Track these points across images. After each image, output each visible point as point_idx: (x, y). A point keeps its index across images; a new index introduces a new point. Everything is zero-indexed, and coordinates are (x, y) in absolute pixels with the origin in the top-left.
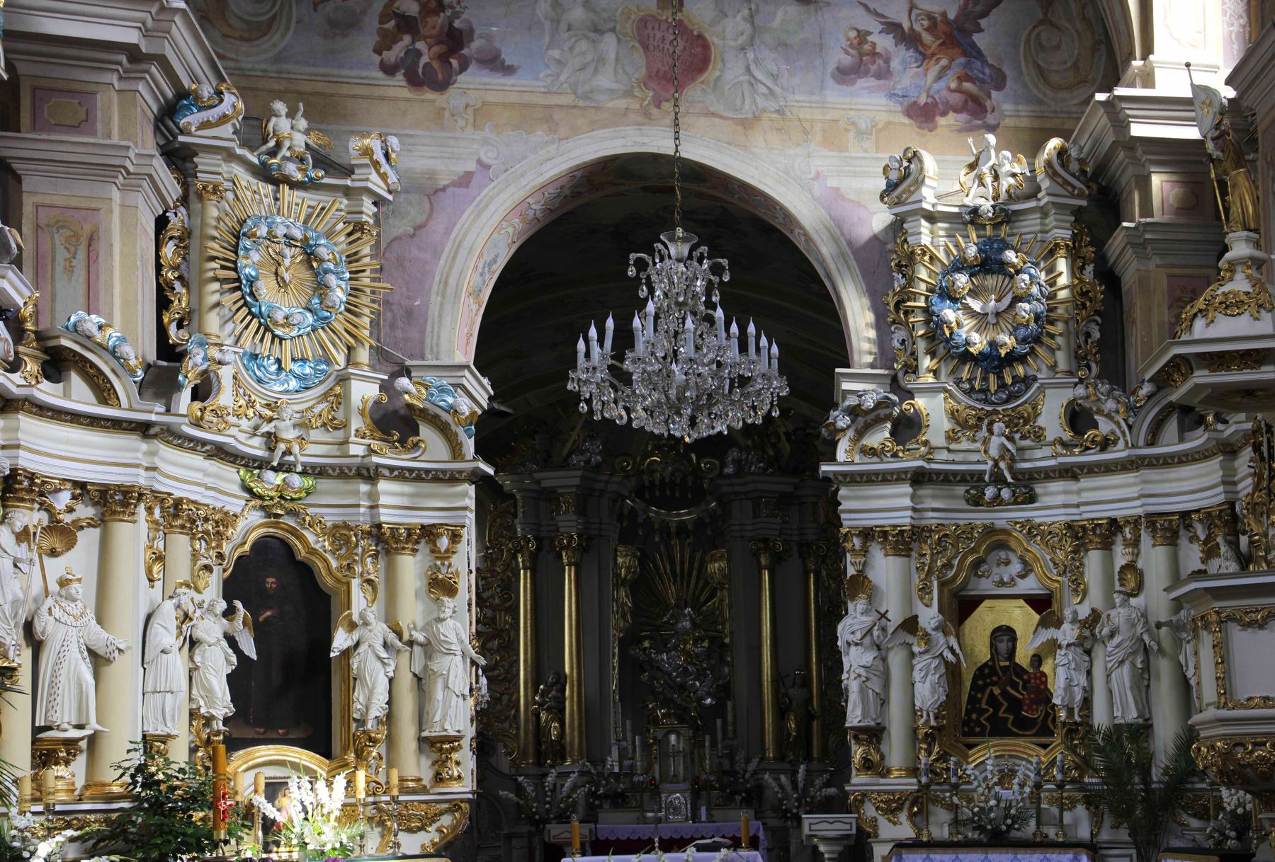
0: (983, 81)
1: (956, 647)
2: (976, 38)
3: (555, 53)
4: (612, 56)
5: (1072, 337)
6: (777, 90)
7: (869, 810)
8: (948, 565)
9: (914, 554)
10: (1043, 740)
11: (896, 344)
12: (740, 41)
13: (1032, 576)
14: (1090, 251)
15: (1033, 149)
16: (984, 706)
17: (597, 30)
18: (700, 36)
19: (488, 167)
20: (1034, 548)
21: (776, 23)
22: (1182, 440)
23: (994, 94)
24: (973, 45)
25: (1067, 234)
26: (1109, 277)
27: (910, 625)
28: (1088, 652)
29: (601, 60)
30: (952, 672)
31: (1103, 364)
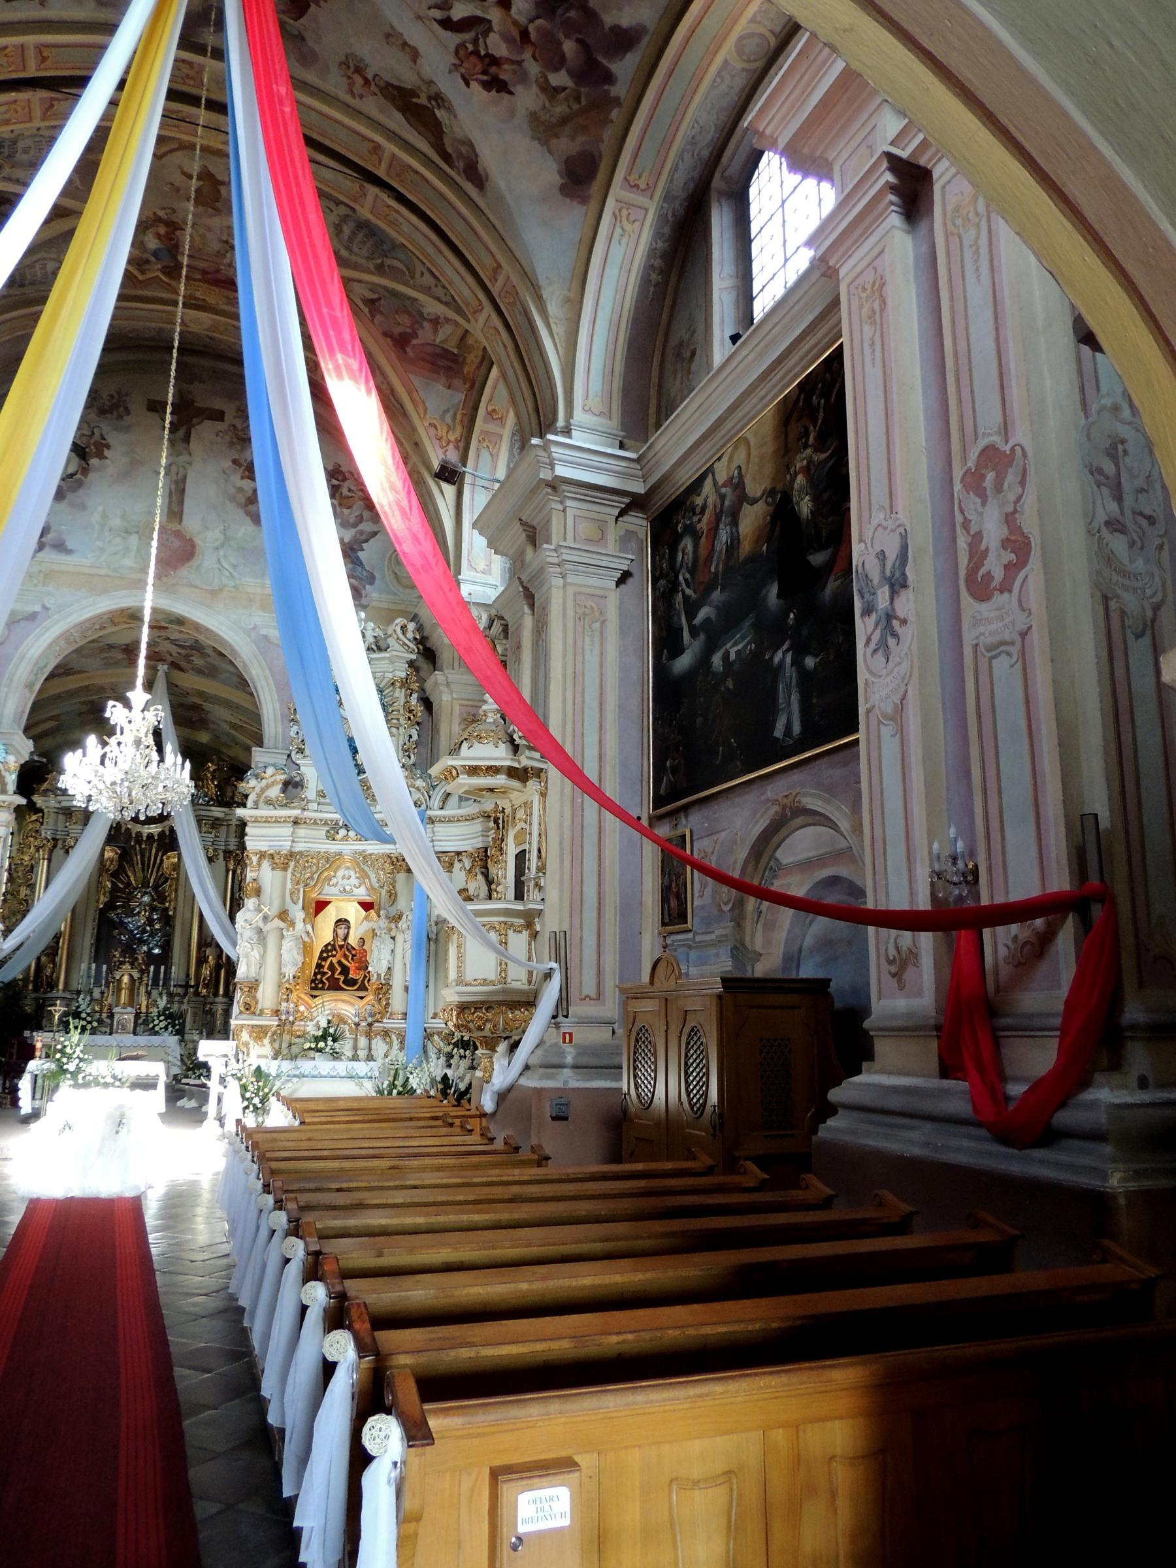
0: (361, 579)
1: (311, 931)
2: (360, 554)
3: (99, 544)
4: (135, 548)
5: (401, 738)
6: (235, 574)
7: (245, 1036)
8: (311, 878)
9: (290, 870)
10: (362, 994)
11: (293, 734)
12: (216, 544)
13: (363, 887)
14: (415, 686)
15: (390, 621)
16: (325, 970)
17: (127, 532)
18: (191, 540)
19: (46, 609)
20: (367, 869)
21: (240, 535)
22: (459, 807)
23: (368, 587)
24: (358, 558)
25: (403, 675)
26: (427, 704)
27: (283, 915)
28: (393, 938)
29: (127, 550)
30: (306, 948)
31: (418, 755)
